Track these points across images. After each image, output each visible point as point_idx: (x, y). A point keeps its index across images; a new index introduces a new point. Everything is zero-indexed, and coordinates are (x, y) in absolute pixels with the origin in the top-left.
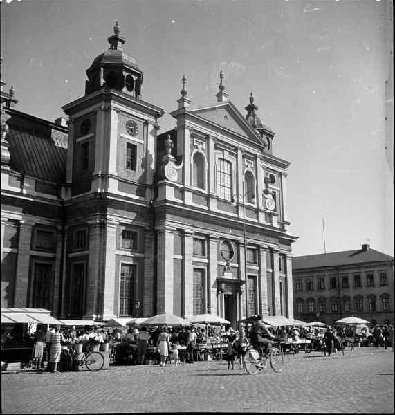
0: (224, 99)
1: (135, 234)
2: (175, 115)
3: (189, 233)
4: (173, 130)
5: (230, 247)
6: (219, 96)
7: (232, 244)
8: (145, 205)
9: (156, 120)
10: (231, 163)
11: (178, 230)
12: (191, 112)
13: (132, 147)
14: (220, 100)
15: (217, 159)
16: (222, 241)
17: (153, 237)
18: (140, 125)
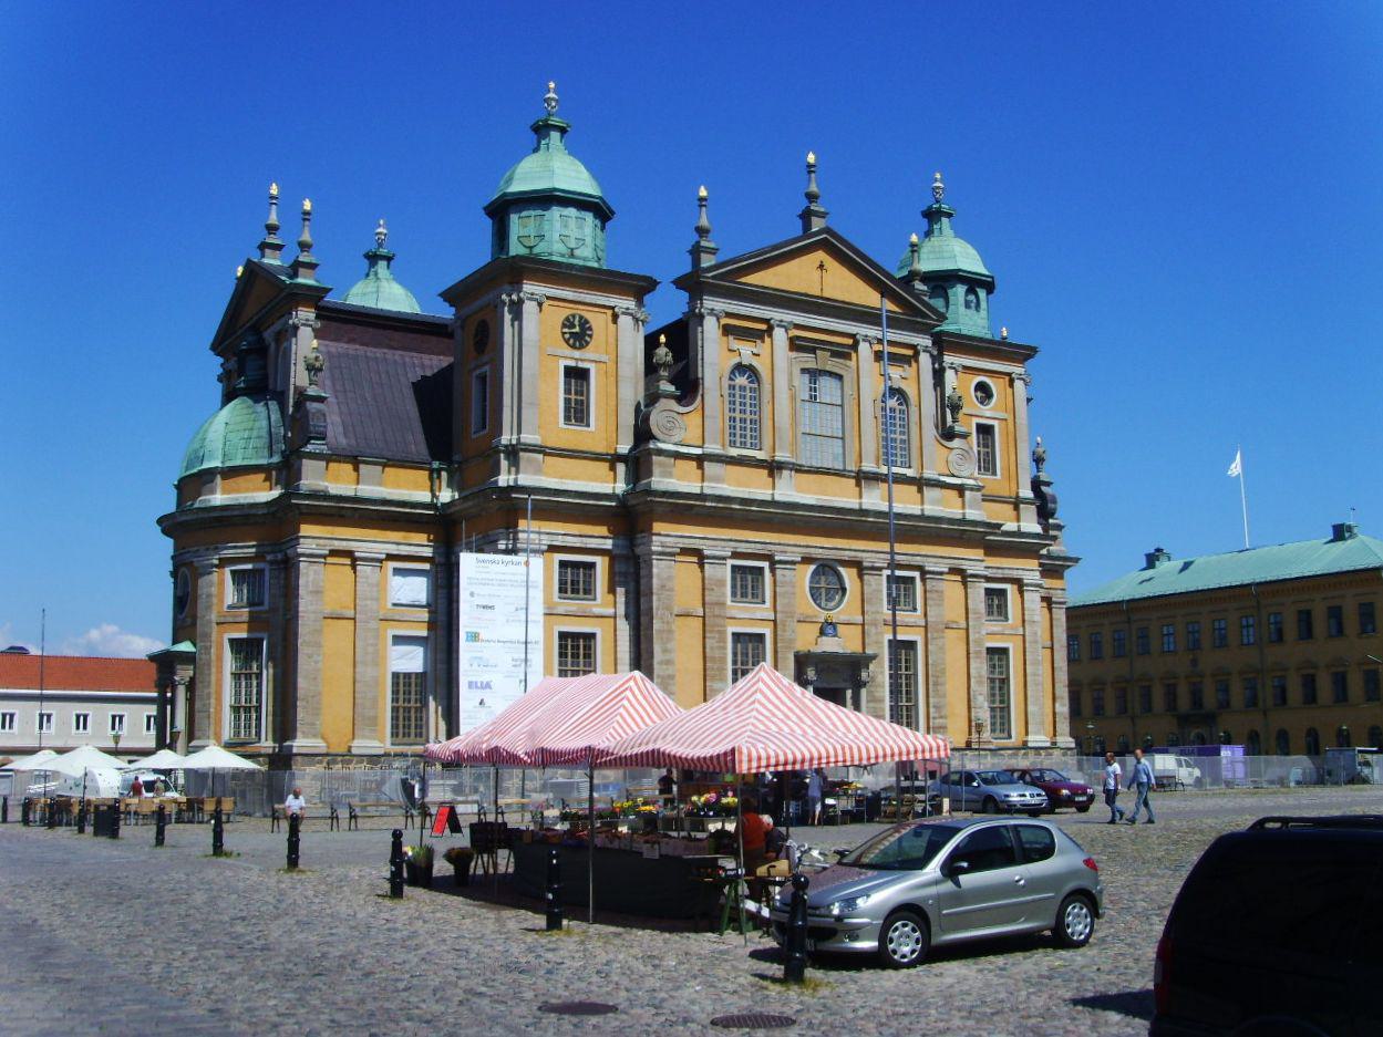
0: (817, 224)
1: (592, 565)
2: (680, 283)
3: (714, 557)
4: (679, 322)
5: (840, 577)
6: (806, 216)
7: (841, 569)
8: (614, 504)
9: (640, 303)
10: (840, 377)
11: (685, 551)
12: (713, 277)
13: (577, 375)
14: (807, 226)
15: (796, 371)
16: (813, 567)
17: (632, 570)
18: (598, 321)
